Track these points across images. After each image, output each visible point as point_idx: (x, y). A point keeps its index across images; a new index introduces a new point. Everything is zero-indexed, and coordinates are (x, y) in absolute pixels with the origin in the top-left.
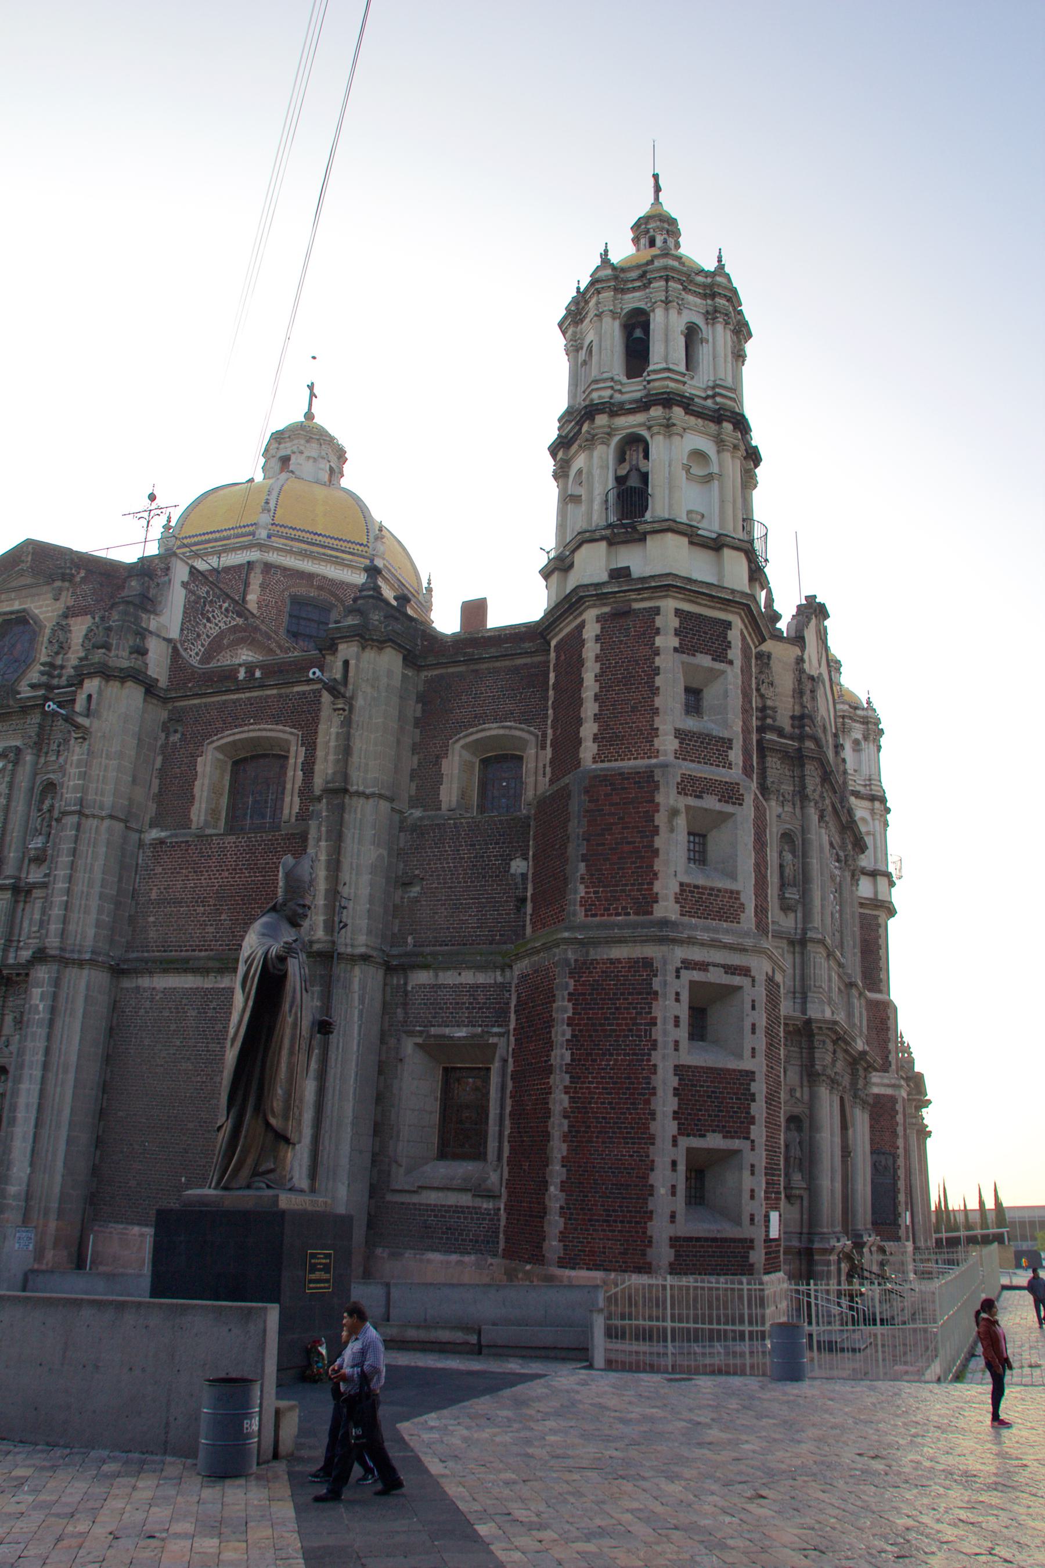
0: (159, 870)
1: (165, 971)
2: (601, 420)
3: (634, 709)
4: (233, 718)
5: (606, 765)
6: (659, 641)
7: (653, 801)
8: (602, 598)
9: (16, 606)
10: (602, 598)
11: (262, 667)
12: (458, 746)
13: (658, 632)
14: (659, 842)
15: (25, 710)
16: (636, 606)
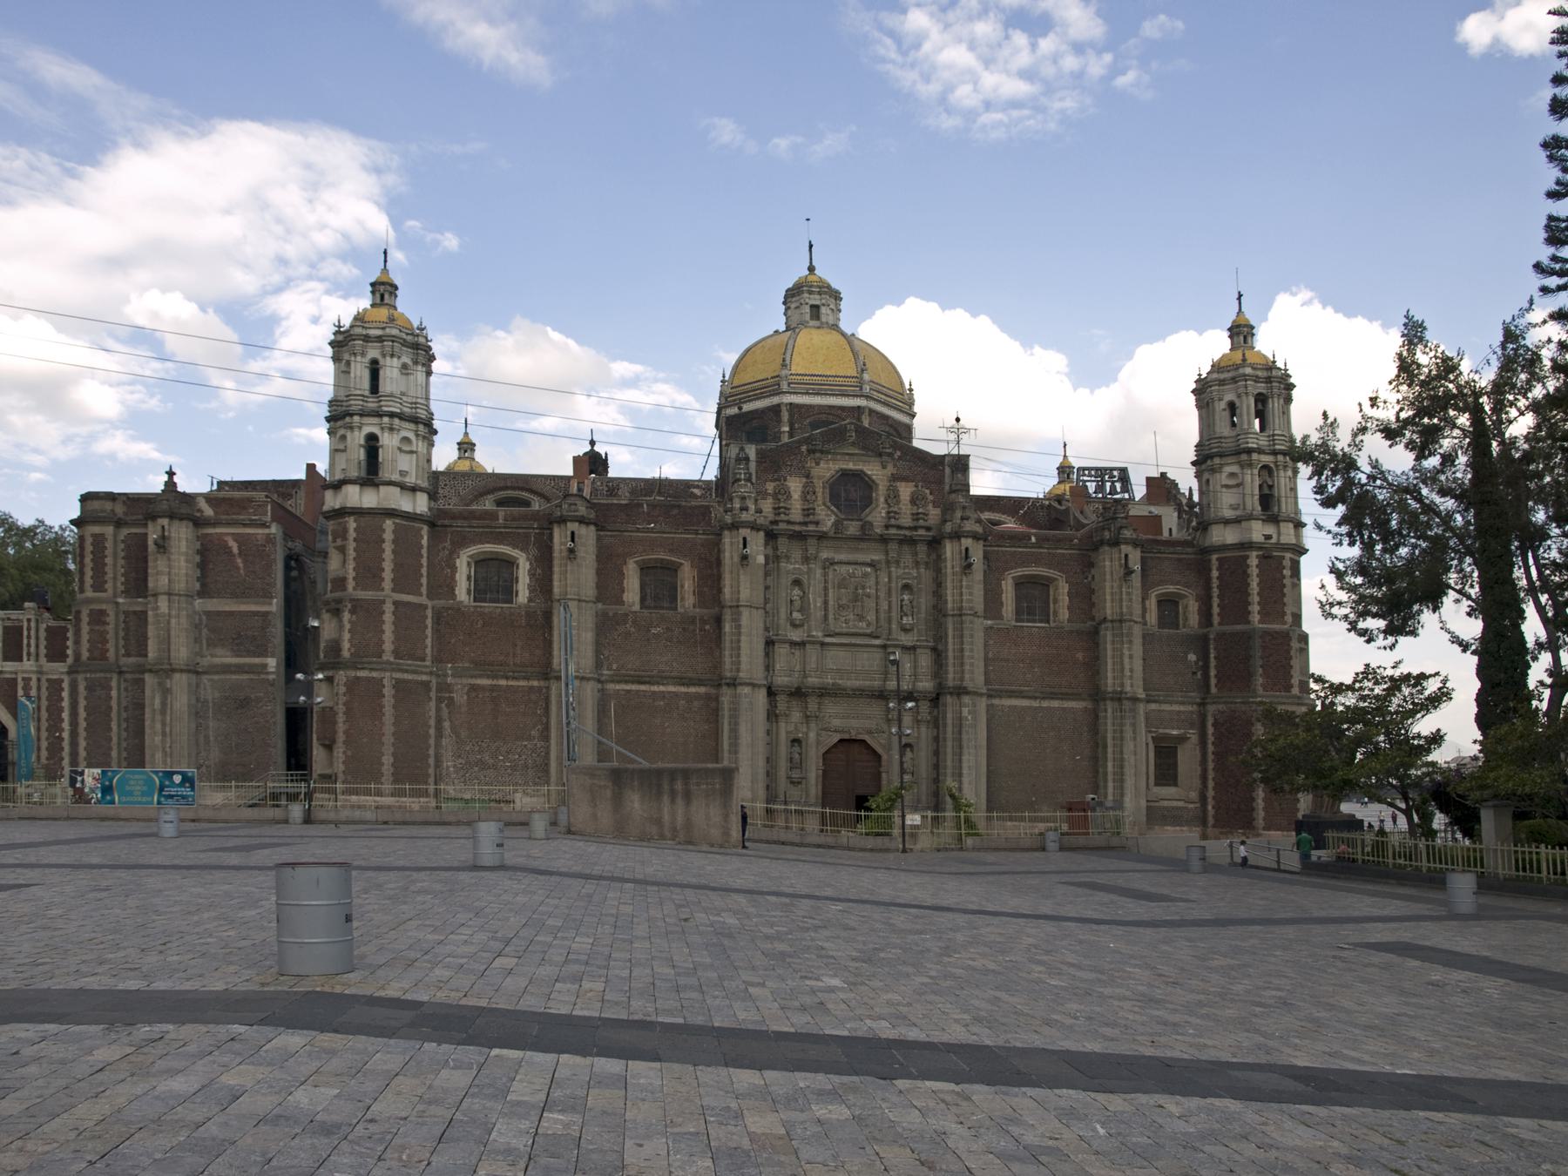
0: (992, 642)
1: (1010, 697)
2: (1255, 456)
3: (1275, 602)
4: (1025, 561)
5: (1265, 626)
6: (1285, 572)
7: (1289, 645)
8: (1260, 548)
9: (851, 466)
10: (1260, 548)
11: (1035, 535)
12: (1153, 595)
13: (1284, 568)
14: (1292, 663)
15: (884, 540)
16: (1275, 554)
